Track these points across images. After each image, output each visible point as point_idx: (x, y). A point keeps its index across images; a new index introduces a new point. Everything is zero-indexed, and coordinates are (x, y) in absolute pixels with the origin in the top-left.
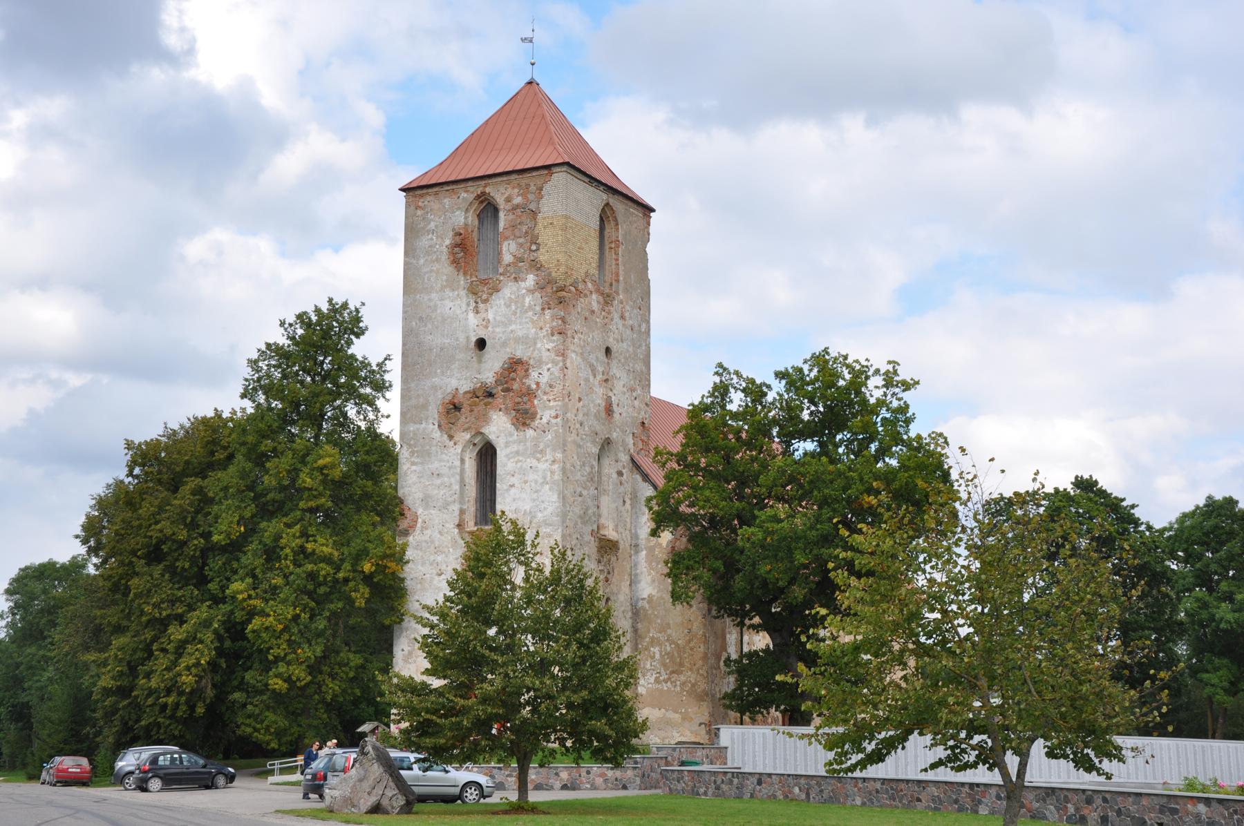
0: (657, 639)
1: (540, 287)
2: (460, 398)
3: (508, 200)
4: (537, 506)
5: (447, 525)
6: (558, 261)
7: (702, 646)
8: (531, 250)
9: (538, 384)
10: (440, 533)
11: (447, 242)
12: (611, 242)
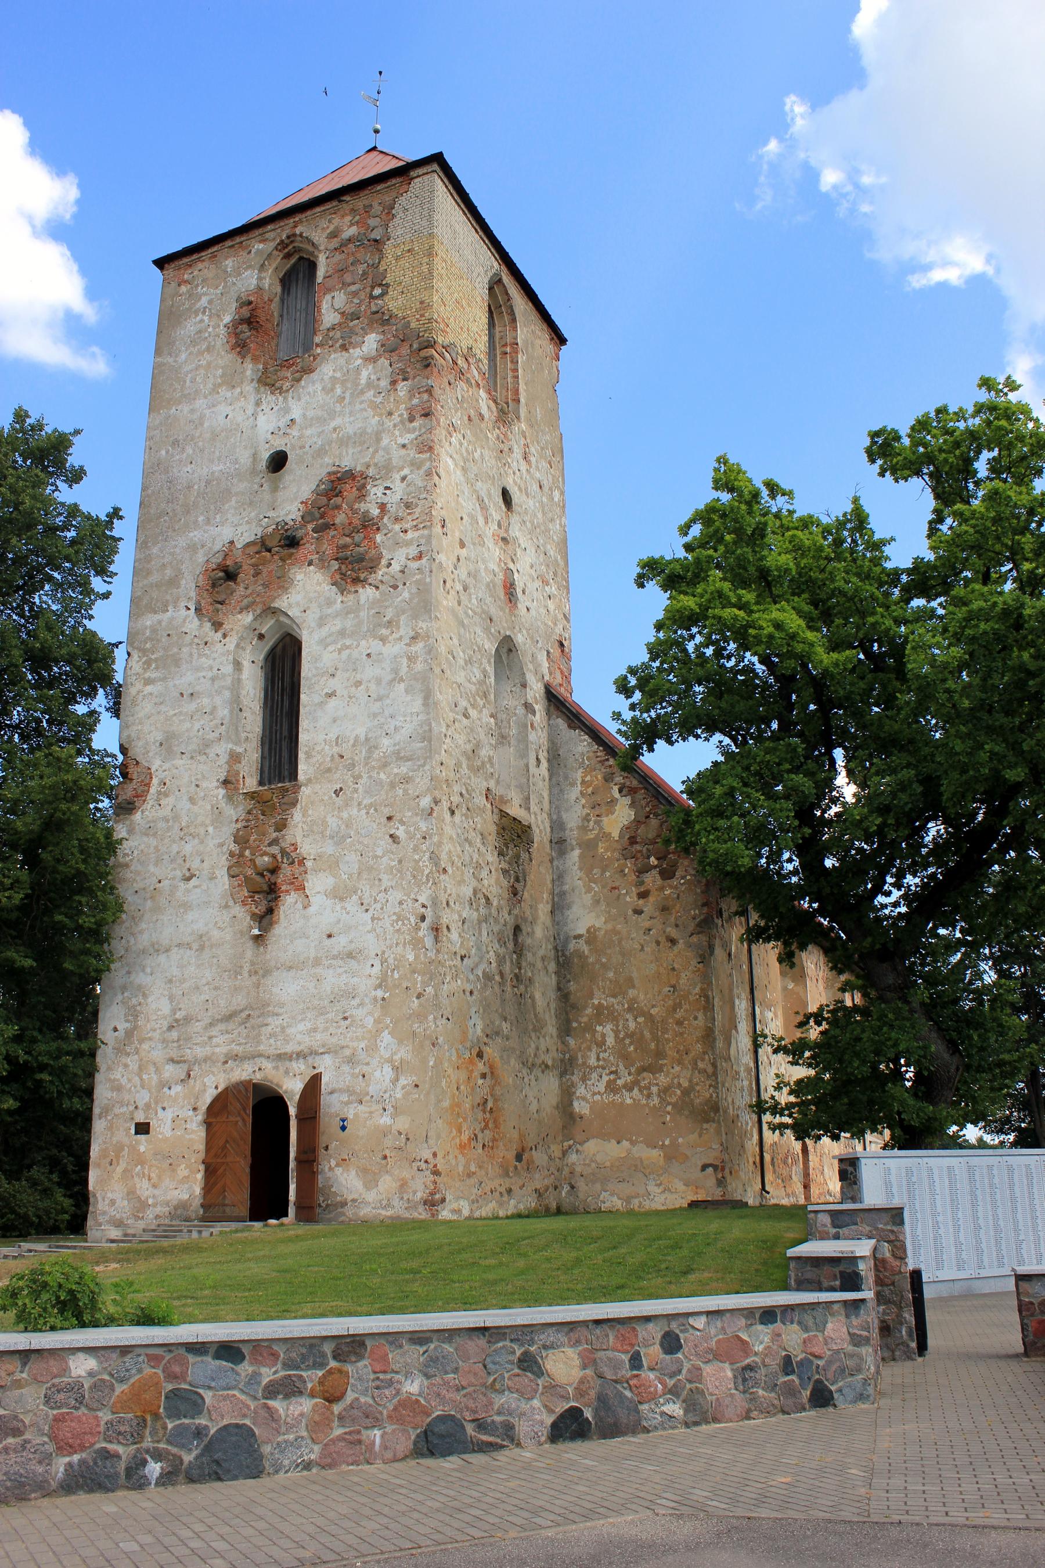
0: (607, 1008)
1: (387, 349)
2: (238, 556)
3: (334, 235)
4: (381, 726)
5: (204, 784)
6: (422, 303)
7: (700, 1016)
8: (372, 297)
9: (383, 507)
10: (192, 800)
11: (227, 319)
12: (505, 345)
